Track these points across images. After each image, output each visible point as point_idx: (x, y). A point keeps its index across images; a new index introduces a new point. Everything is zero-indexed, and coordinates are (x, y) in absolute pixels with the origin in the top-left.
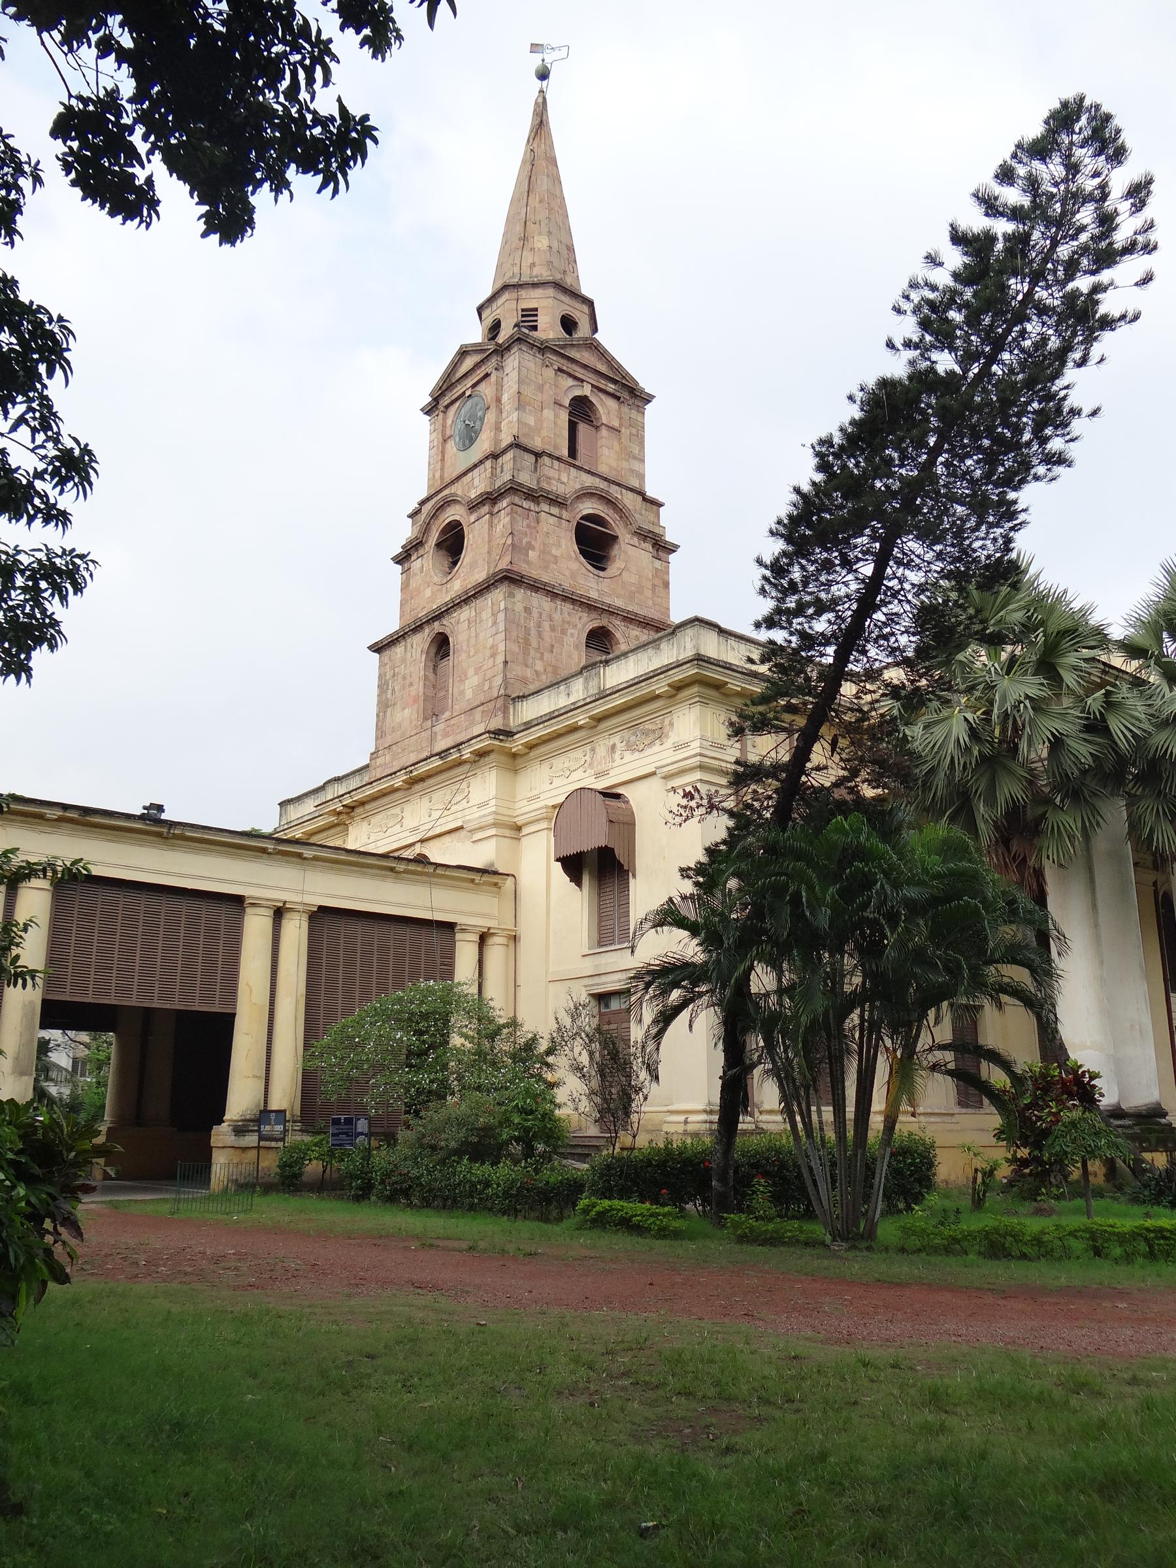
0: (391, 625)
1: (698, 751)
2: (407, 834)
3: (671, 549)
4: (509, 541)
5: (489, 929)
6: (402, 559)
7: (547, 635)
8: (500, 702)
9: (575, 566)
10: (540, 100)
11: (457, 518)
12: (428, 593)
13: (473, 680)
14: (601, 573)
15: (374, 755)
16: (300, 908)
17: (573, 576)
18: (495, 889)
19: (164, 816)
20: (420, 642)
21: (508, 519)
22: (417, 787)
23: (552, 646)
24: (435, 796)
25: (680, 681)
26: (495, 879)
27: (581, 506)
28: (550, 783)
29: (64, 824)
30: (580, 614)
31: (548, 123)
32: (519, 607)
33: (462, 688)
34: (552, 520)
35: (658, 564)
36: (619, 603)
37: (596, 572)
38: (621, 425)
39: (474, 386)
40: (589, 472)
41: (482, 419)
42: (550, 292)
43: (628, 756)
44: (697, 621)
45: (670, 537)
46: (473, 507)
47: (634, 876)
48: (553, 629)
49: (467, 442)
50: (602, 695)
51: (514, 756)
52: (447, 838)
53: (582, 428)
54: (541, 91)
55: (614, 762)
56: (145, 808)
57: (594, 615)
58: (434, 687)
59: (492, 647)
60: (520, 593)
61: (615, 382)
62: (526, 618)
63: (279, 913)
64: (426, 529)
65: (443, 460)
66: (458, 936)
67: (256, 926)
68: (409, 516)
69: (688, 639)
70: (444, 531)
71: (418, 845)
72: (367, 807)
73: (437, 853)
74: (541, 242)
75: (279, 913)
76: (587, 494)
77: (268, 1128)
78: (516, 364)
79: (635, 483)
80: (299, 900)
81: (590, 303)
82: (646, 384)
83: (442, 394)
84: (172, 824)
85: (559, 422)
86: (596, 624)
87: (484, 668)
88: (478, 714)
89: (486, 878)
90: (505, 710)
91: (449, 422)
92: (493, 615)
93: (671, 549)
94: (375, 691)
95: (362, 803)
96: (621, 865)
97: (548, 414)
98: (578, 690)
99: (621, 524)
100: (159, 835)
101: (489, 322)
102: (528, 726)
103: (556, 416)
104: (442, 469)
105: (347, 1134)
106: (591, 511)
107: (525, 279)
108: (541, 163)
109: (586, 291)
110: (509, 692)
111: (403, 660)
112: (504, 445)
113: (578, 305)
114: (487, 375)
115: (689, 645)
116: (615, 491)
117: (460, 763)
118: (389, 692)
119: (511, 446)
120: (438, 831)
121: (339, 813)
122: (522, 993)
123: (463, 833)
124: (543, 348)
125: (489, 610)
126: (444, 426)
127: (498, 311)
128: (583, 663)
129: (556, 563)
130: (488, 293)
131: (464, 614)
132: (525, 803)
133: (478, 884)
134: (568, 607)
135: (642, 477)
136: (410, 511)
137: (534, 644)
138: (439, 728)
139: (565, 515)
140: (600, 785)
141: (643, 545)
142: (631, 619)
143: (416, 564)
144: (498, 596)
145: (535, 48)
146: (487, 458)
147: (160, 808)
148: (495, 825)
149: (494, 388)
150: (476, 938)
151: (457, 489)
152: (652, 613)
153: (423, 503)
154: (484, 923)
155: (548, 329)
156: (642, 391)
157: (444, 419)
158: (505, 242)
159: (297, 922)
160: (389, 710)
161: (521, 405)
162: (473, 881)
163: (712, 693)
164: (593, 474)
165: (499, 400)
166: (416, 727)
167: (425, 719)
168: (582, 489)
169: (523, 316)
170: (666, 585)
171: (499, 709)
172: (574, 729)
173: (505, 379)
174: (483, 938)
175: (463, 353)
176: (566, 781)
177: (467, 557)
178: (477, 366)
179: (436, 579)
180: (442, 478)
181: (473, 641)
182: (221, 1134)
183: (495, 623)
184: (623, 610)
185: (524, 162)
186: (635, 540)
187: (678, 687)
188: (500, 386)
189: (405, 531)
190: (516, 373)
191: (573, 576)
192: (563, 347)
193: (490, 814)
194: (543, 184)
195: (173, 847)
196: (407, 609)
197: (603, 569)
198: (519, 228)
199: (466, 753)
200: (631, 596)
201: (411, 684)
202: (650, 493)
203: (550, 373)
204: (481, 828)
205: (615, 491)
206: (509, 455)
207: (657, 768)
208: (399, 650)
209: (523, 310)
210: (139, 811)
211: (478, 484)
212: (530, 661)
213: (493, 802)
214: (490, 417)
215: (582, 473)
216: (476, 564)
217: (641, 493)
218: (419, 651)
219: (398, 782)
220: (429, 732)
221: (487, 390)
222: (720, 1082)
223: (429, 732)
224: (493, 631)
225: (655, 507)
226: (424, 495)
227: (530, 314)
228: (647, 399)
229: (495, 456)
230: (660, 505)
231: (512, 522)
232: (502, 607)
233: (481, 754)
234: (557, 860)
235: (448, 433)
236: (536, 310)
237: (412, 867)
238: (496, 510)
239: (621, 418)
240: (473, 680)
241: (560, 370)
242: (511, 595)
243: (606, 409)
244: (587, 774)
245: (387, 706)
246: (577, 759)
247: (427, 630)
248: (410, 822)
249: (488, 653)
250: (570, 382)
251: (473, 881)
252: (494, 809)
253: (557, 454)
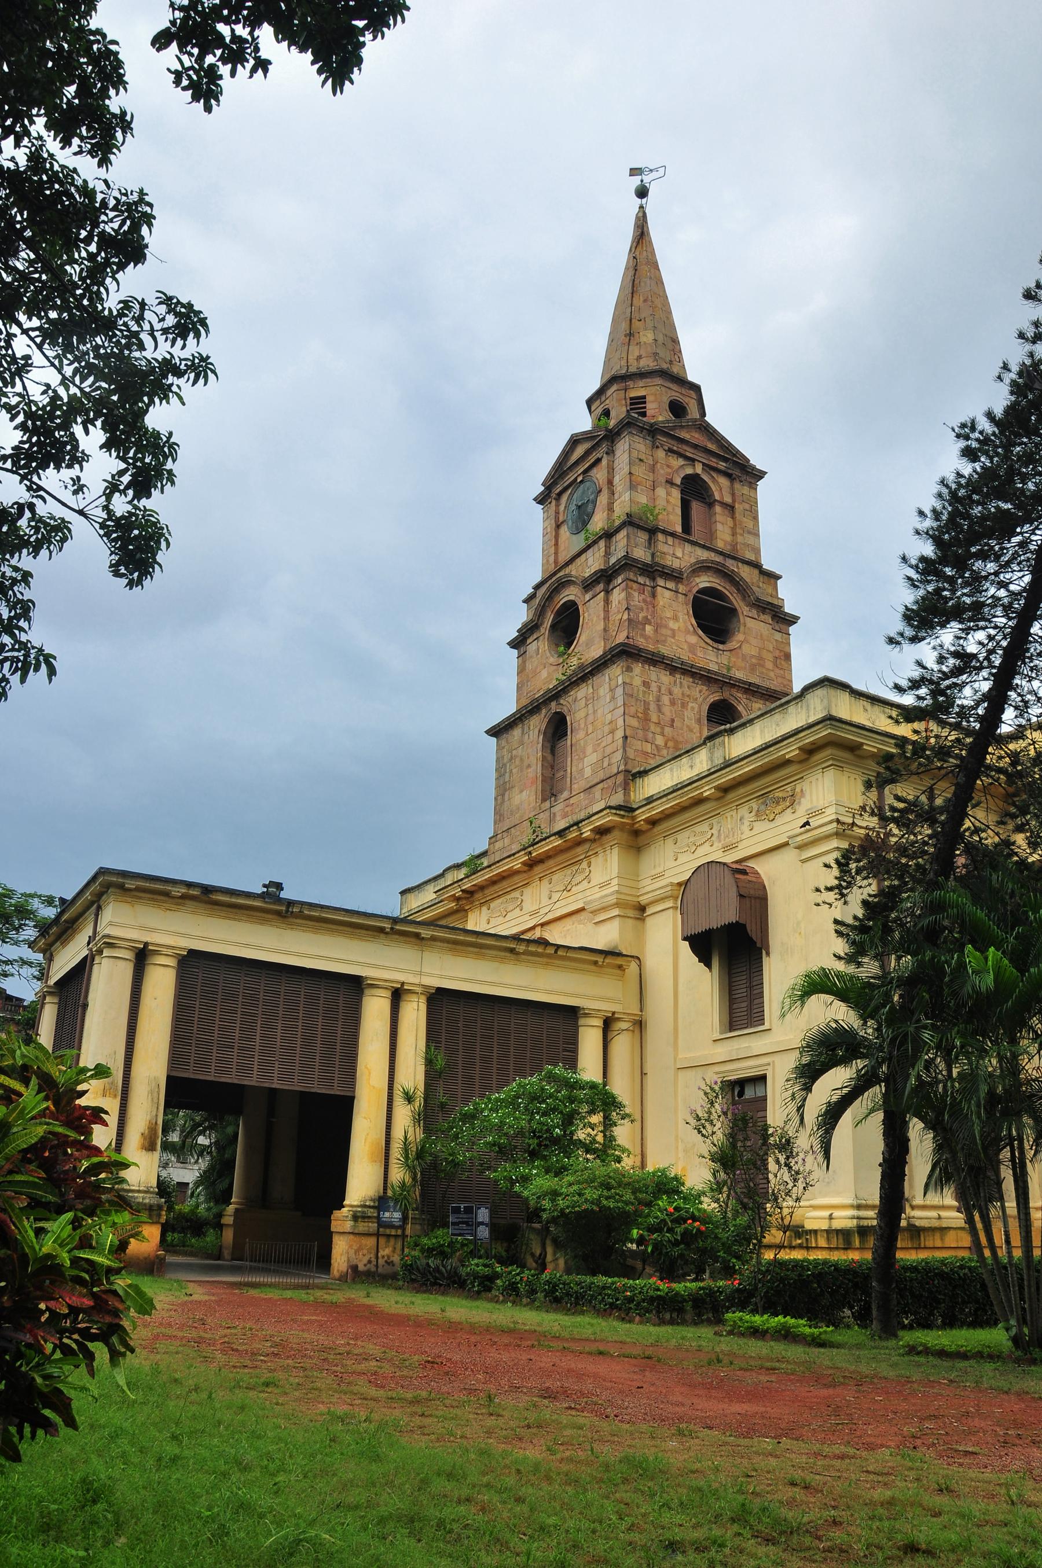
0: (509, 707)
1: (834, 817)
2: (527, 917)
3: (792, 620)
4: (626, 617)
5: (614, 1013)
6: (519, 643)
7: (667, 710)
8: (620, 778)
9: (693, 639)
10: (641, 214)
11: (572, 598)
12: (544, 674)
13: (591, 758)
14: (721, 647)
15: (493, 839)
16: (419, 990)
17: (692, 648)
18: (619, 972)
19: (283, 895)
20: (537, 723)
21: (623, 595)
22: (538, 869)
23: (673, 721)
24: (555, 877)
25: (812, 743)
26: (619, 961)
27: (697, 580)
28: (674, 861)
29: (187, 902)
30: (699, 687)
31: (648, 234)
32: (637, 681)
34: (667, 594)
35: (778, 636)
36: (739, 675)
37: (715, 645)
38: (734, 501)
40: (704, 547)
41: (594, 502)
42: (658, 381)
43: (759, 826)
44: (827, 682)
45: (788, 609)
46: (588, 585)
47: (768, 954)
48: (673, 703)
49: (580, 525)
50: (728, 764)
51: (636, 833)
52: (568, 922)
53: (696, 507)
54: (641, 207)
55: (742, 834)
56: (265, 886)
57: (715, 687)
58: (552, 767)
59: (611, 722)
60: (638, 668)
61: (726, 460)
62: (645, 692)
63: (397, 995)
64: (541, 612)
65: (556, 544)
66: (581, 1022)
67: (375, 1009)
68: (524, 601)
69: (817, 701)
70: (558, 613)
71: (538, 930)
72: (486, 892)
73: (556, 936)
74: (647, 337)
75: (397, 995)
76: (702, 568)
77: (387, 1214)
78: (627, 447)
79: (750, 556)
80: (416, 981)
81: (696, 388)
82: (756, 460)
83: (555, 483)
84: (290, 903)
85: (672, 500)
86: (715, 697)
87: (603, 744)
88: (597, 791)
89: (609, 960)
90: (626, 787)
91: (562, 508)
92: (611, 690)
93: (792, 620)
94: (494, 775)
95: (481, 888)
96: (753, 942)
97: (661, 492)
98: (701, 762)
99: (739, 598)
100: (278, 913)
101: (600, 410)
102: (650, 800)
103: (668, 494)
104: (556, 553)
105: (467, 1223)
106: (708, 585)
107: (633, 369)
108: (644, 269)
109: (692, 377)
110: (629, 767)
111: (522, 743)
112: (617, 523)
113: (684, 391)
114: (598, 461)
115: (819, 707)
116: (730, 564)
117: (579, 842)
118: (507, 775)
119: (623, 525)
120: (558, 914)
121: (458, 899)
122: (650, 1081)
123: (583, 916)
124: (653, 432)
125: (607, 686)
126: (557, 513)
127: (607, 402)
128: (706, 733)
129: (673, 637)
130: (596, 386)
131: (582, 692)
132: (648, 881)
133: (601, 967)
134: (687, 681)
135: (757, 551)
136: (525, 596)
137: (654, 718)
138: (558, 809)
139: (682, 588)
140: (729, 858)
141: (763, 617)
142: (752, 690)
143: (532, 647)
144: (615, 672)
145: (634, 172)
146: (600, 538)
147: (279, 886)
148: (617, 905)
149: (606, 471)
150: (599, 1023)
151: (573, 570)
152: (774, 685)
153: (537, 587)
154: (608, 1007)
155: (657, 412)
156: (754, 468)
157: (558, 506)
158: (611, 340)
159: (415, 1005)
161: (633, 487)
162: (596, 963)
163: (846, 755)
164: (708, 549)
165: (610, 482)
166: (535, 808)
167: (544, 800)
168: (698, 562)
169: (631, 404)
170: (788, 657)
171: (620, 785)
172: (699, 801)
173: (616, 462)
174: (608, 1024)
175: (574, 441)
176: (693, 857)
177: (583, 636)
178: (588, 453)
179: (552, 660)
180: (556, 562)
181: (591, 718)
182: (341, 1220)
183: (613, 698)
184: (745, 683)
185: (627, 268)
186: (754, 613)
187: (810, 751)
188: (611, 470)
189: (521, 615)
190: (626, 455)
191: (692, 648)
192: (674, 428)
193: (612, 894)
194: (645, 288)
195: (292, 926)
196: (525, 690)
197: (723, 643)
198: (624, 326)
199: (587, 832)
200: (753, 668)
201: (529, 766)
202: (767, 565)
203: (661, 454)
204: (604, 909)
205: (730, 564)
206: (623, 533)
207: (790, 838)
208: (517, 732)
209: (631, 399)
210: (260, 890)
211: (593, 563)
212: (650, 735)
213: (615, 882)
214: (603, 499)
215: (697, 548)
216: (590, 645)
217: (757, 565)
219: (516, 864)
220: (547, 813)
221: (599, 475)
222: (880, 1169)
223: (547, 813)
224: (612, 706)
225: (772, 581)
226: (538, 579)
227: (638, 403)
228: (760, 475)
229: (608, 535)
230: (779, 577)
231: (629, 597)
232: (620, 681)
233: (602, 832)
234: (685, 939)
235: (561, 519)
236: (644, 397)
237: (532, 948)
238: (611, 587)
239: (733, 495)
240: (591, 758)
241: (670, 451)
242: (629, 669)
243: (720, 487)
244: (714, 848)
245: (505, 790)
246: (703, 833)
247: (544, 711)
248: (529, 905)
249: (607, 729)
250: (681, 462)
251: (596, 963)
252: (616, 888)
253: (670, 529)
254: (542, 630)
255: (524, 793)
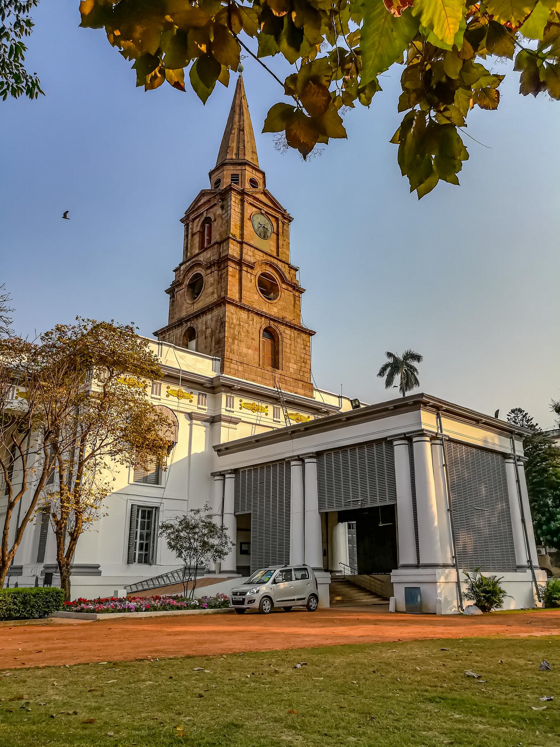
33: (287, 364)
39: (266, 212)
131: (288, 331)
160: (236, 342)
201: (253, 339)
218: (258, 326)
254: (254, 272)
255: (250, 351)
